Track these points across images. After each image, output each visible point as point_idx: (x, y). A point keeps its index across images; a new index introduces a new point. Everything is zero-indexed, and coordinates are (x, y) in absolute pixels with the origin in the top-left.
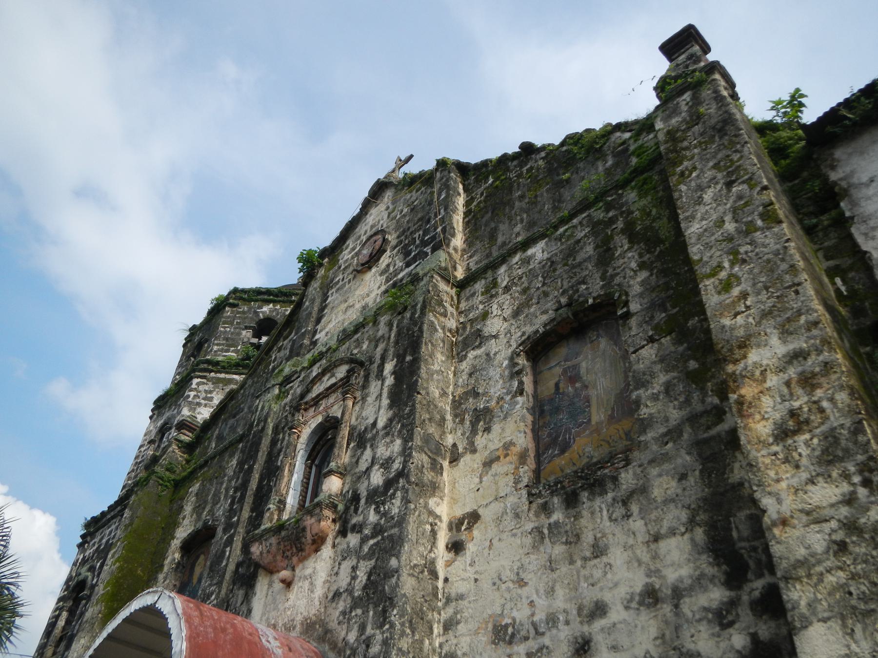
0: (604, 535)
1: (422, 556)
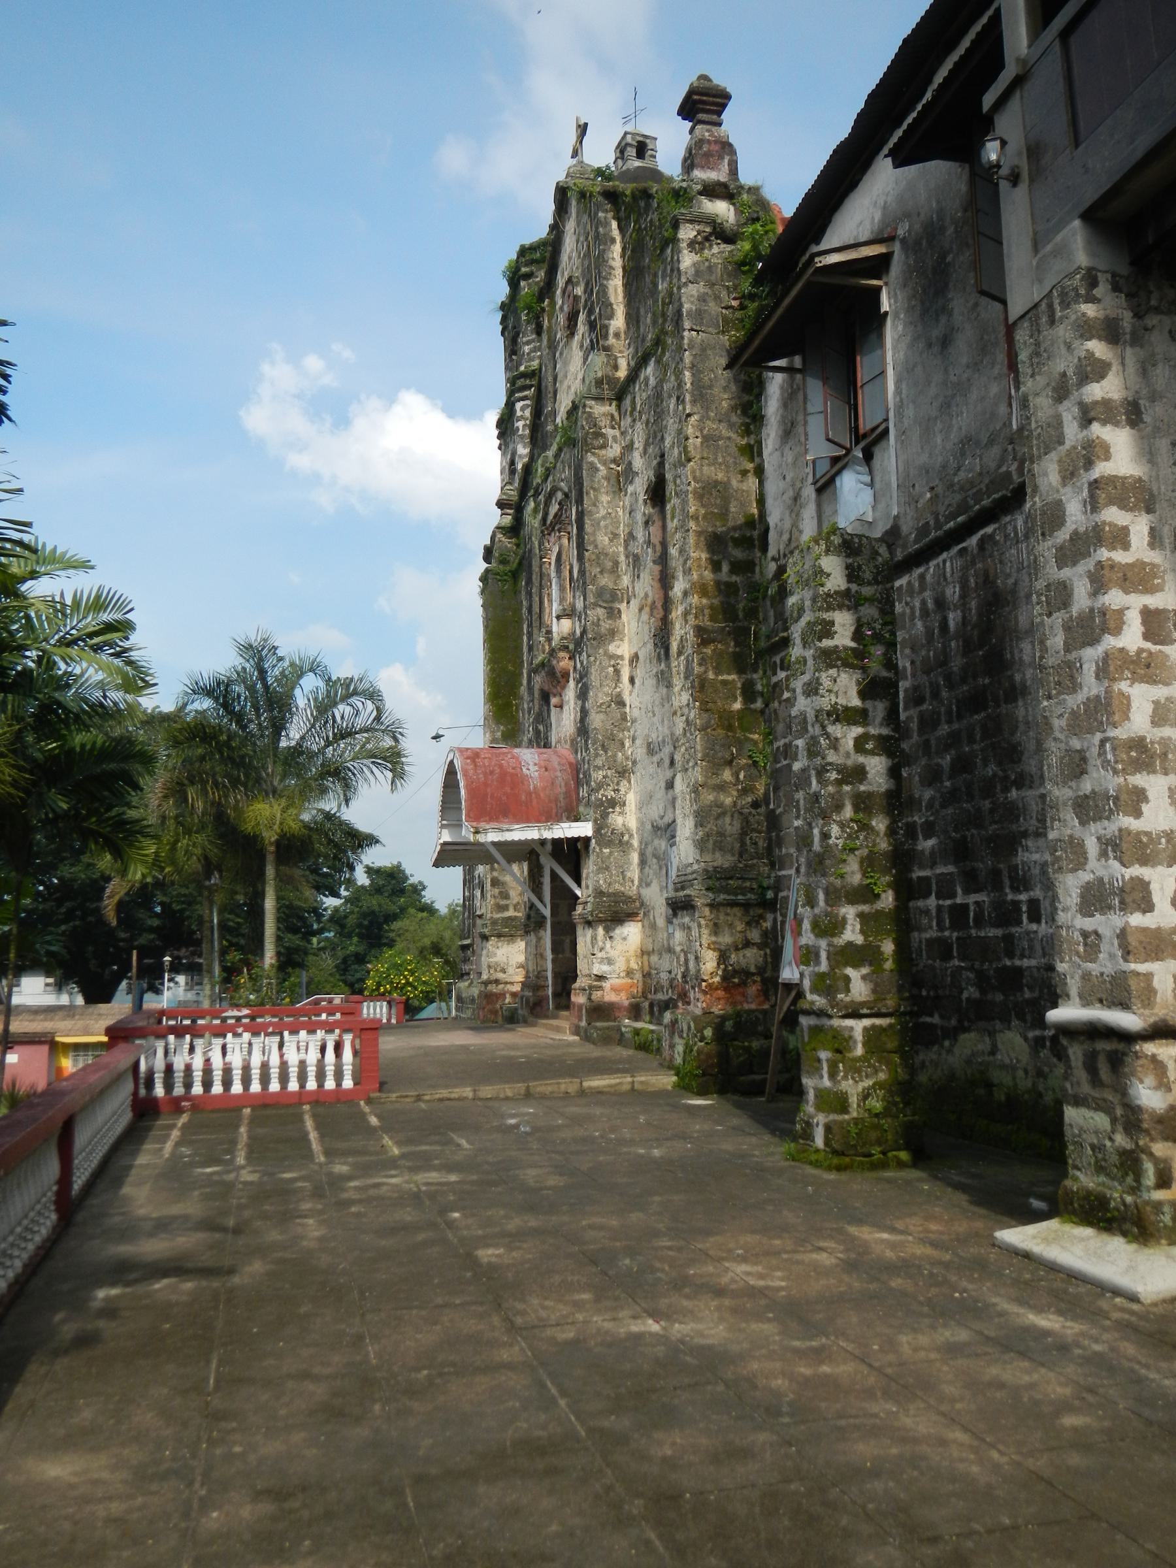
1: (607, 695)
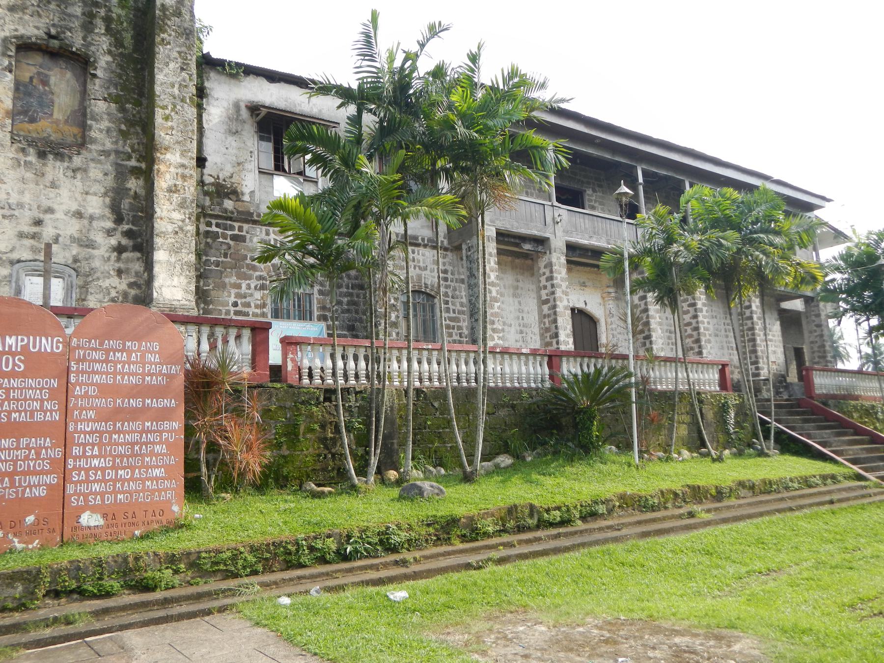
0: (58, 180)
